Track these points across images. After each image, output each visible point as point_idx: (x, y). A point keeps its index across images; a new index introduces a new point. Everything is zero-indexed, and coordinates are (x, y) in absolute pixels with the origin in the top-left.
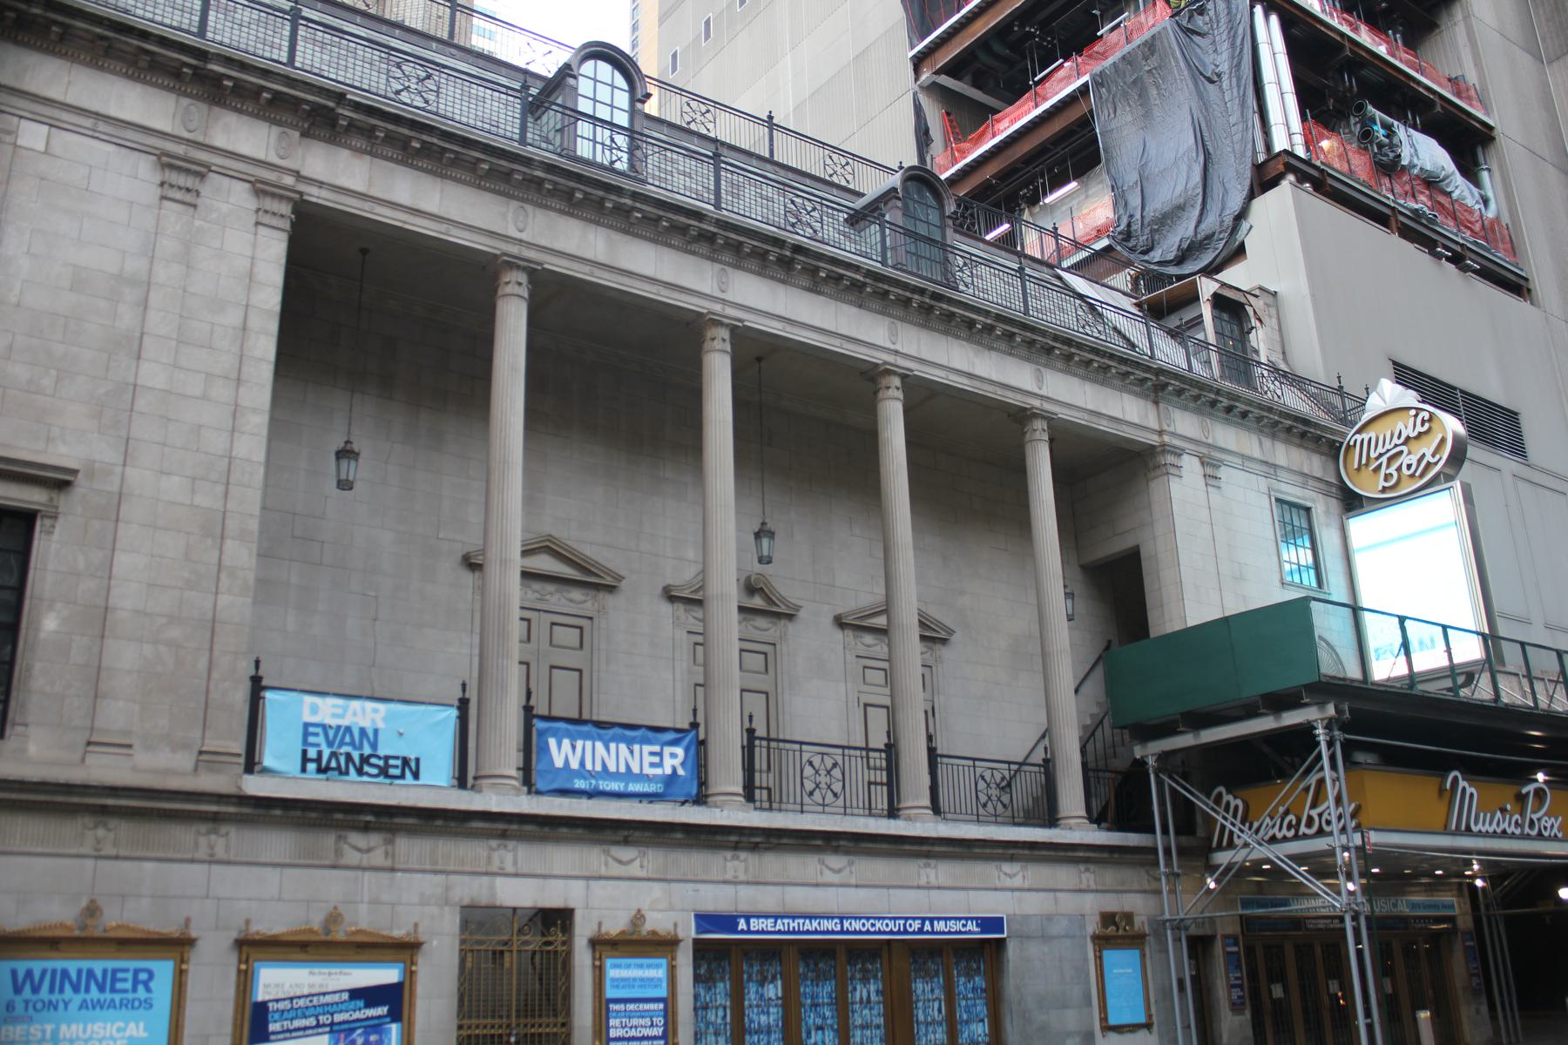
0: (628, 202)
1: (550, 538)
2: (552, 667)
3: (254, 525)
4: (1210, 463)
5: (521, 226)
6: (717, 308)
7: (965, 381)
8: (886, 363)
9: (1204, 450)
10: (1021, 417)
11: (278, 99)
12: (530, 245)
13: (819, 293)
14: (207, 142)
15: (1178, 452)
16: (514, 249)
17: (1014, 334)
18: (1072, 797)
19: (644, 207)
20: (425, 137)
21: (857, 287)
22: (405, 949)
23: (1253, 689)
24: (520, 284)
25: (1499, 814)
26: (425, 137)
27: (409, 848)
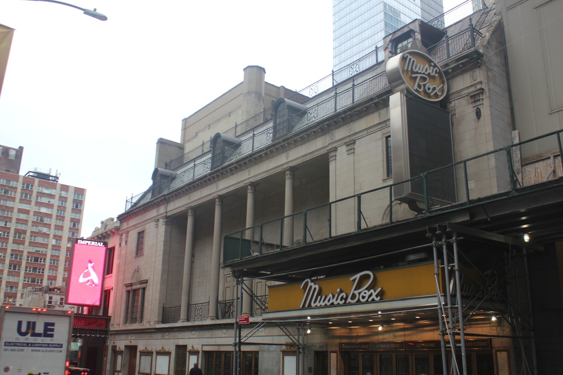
7: (266, 174)
15: (335, 149)
22: (168, 354)
25: (331, 295)
27: (172, 334)
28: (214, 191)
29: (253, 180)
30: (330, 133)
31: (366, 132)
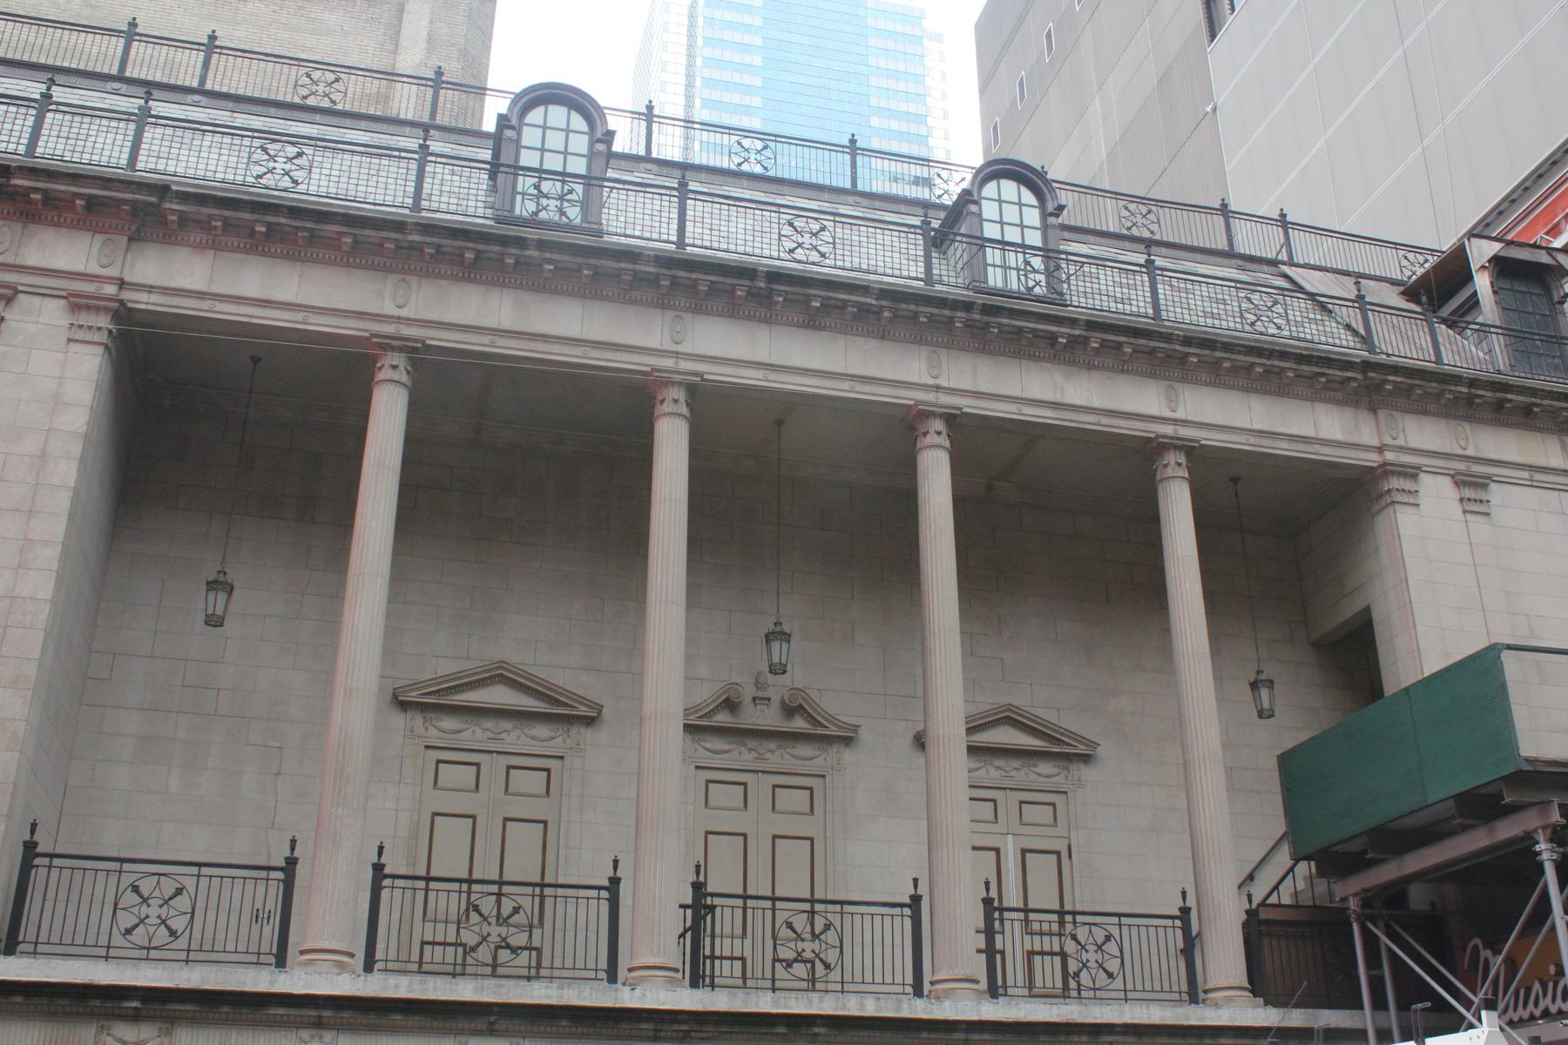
0: (534, 253)
1: (503, 664)
2: (506, 819)
3: (31, 670)
4: (1472, 483)
5: (400, 301)
6: (668, 363)
7: (1049, 413)
8: (918, 402)
9: (1461, 466)
10: (1149, 451)
11: (92, 204)
12: (409, 321)
13: (819, 328)
14: (18, 262)
15: (1412, 473)
16: (390, 329)
17: (1120, 345)
18: (1225, 959)
19: (556, 257)
20: (270, 219)
21: (864, 312)
23: (1443, 788)
24: (394, 367)
26: (270, 219)
28: (653, 343)
29: (970, 406)
30: (1382, 413)
31: (1526, 475)
